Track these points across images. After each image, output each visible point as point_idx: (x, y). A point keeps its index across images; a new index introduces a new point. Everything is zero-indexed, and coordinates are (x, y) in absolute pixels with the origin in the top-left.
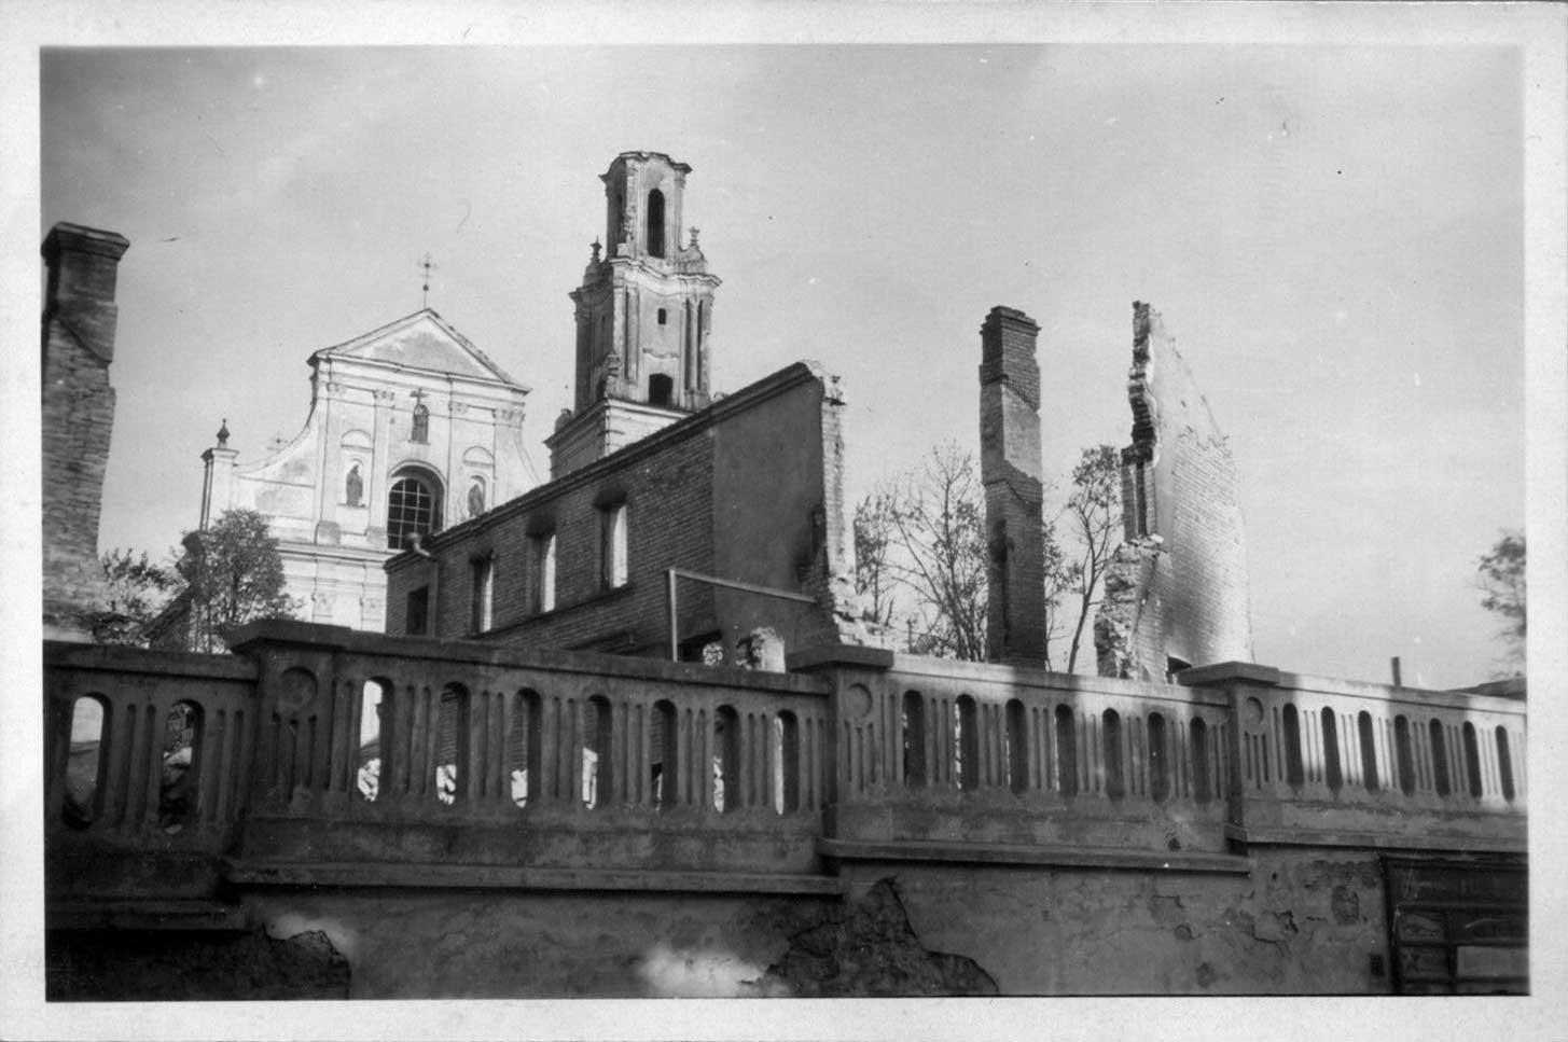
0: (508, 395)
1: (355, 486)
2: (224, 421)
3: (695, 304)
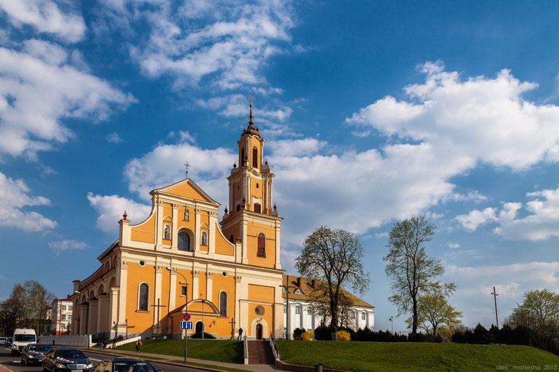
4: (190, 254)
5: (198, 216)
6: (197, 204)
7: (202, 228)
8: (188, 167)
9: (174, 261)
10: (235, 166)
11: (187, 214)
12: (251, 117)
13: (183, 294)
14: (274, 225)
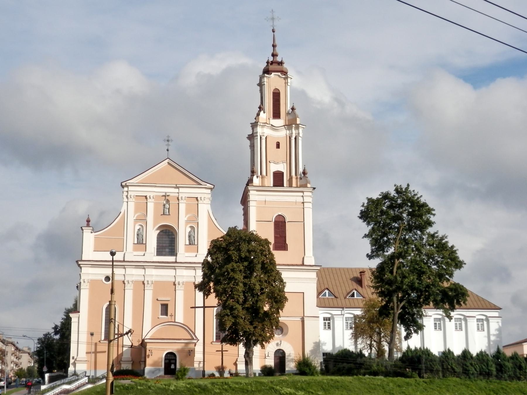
4: (171, 259)
5: (183, 207)
6: (181, 190)
7: (187, 222)
8: (170, 143)
9: (149, 271)
11: (167, 206)
12: (274, 46)
13: (162, 314)
14: (301, 200)
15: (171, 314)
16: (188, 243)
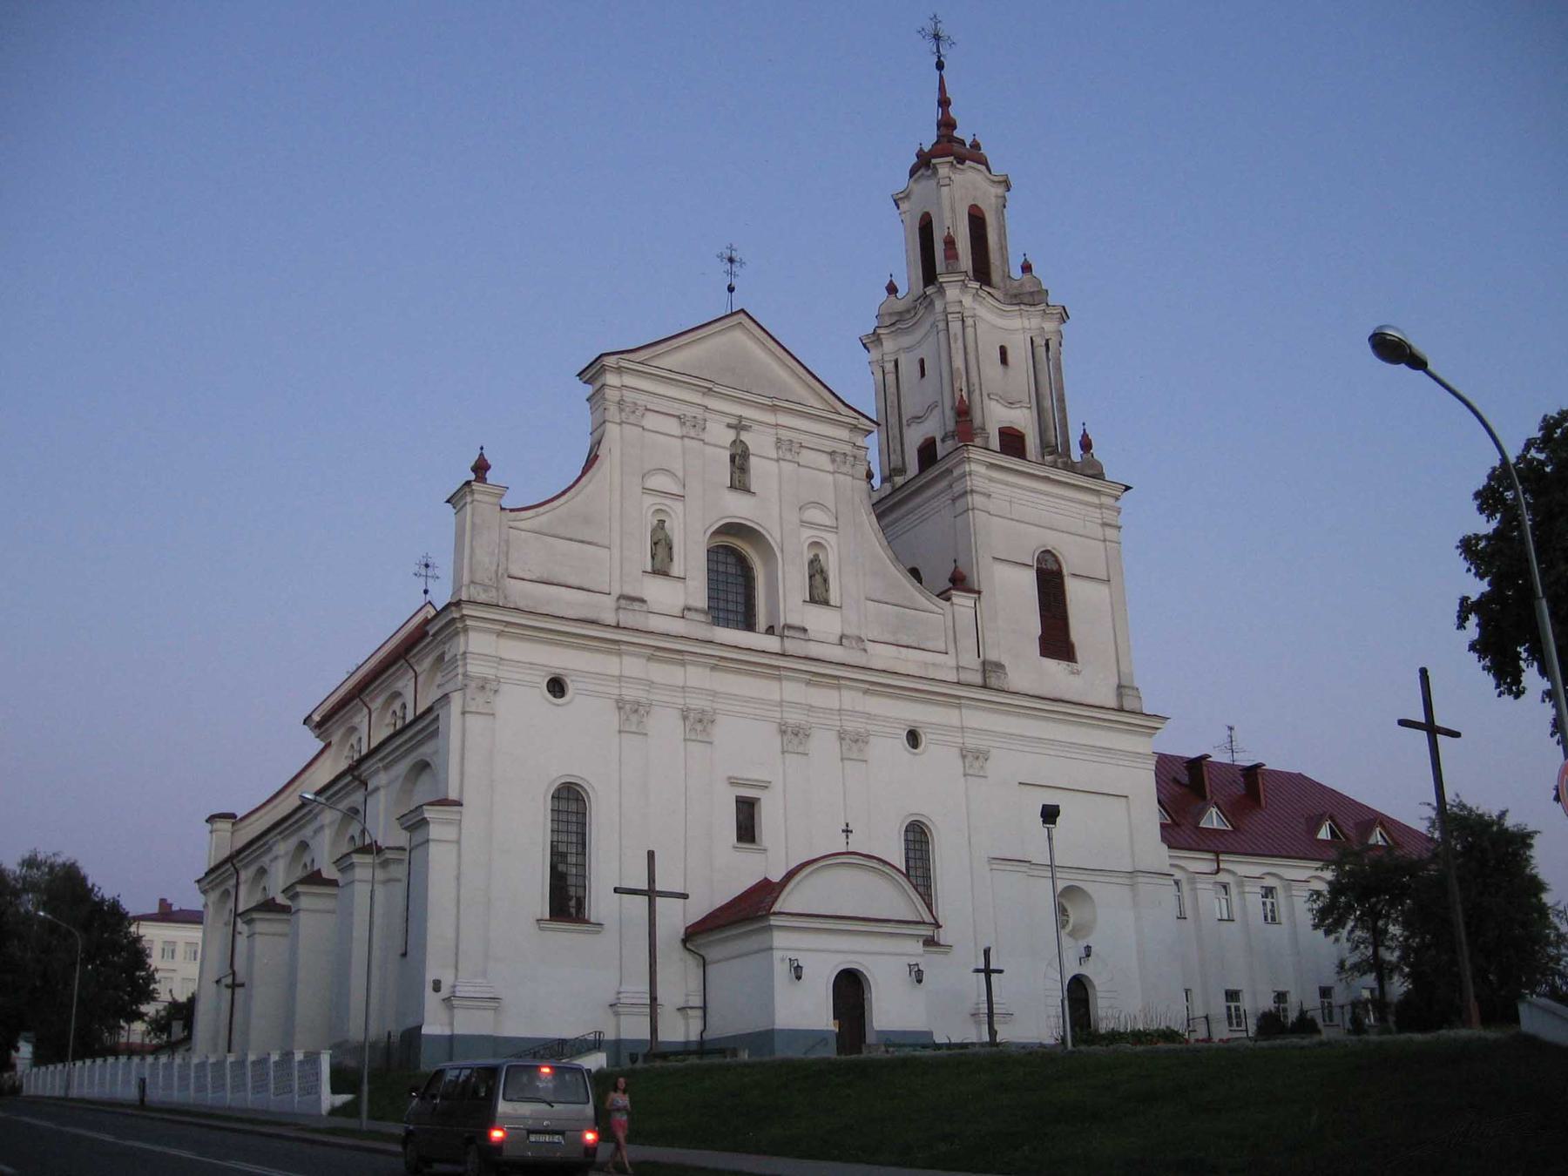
0: (844, 434)
1: (661, 546)
2: (482, 448)
3: (1040, 342)
10: (892, 289)
12: (944, 103)
15: (847, 825)
16: (808, 599)
